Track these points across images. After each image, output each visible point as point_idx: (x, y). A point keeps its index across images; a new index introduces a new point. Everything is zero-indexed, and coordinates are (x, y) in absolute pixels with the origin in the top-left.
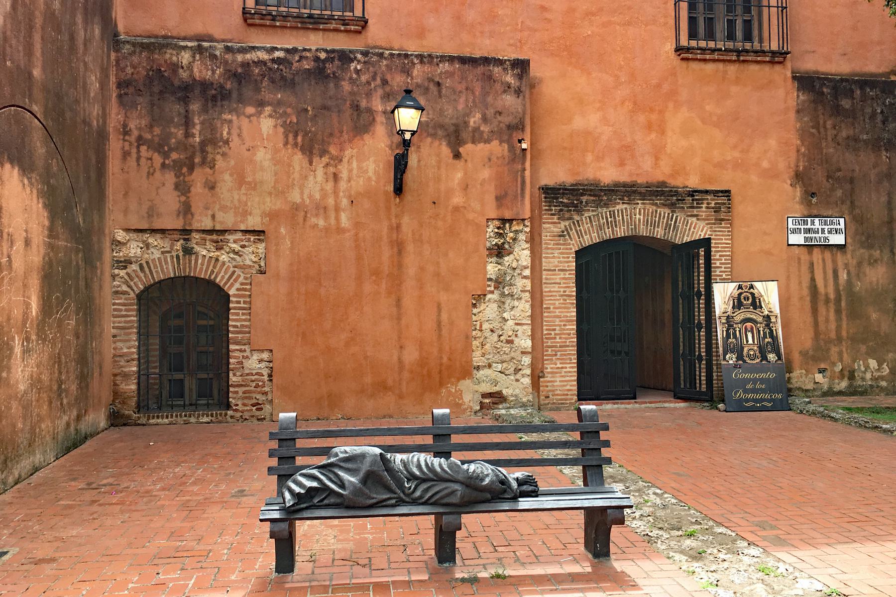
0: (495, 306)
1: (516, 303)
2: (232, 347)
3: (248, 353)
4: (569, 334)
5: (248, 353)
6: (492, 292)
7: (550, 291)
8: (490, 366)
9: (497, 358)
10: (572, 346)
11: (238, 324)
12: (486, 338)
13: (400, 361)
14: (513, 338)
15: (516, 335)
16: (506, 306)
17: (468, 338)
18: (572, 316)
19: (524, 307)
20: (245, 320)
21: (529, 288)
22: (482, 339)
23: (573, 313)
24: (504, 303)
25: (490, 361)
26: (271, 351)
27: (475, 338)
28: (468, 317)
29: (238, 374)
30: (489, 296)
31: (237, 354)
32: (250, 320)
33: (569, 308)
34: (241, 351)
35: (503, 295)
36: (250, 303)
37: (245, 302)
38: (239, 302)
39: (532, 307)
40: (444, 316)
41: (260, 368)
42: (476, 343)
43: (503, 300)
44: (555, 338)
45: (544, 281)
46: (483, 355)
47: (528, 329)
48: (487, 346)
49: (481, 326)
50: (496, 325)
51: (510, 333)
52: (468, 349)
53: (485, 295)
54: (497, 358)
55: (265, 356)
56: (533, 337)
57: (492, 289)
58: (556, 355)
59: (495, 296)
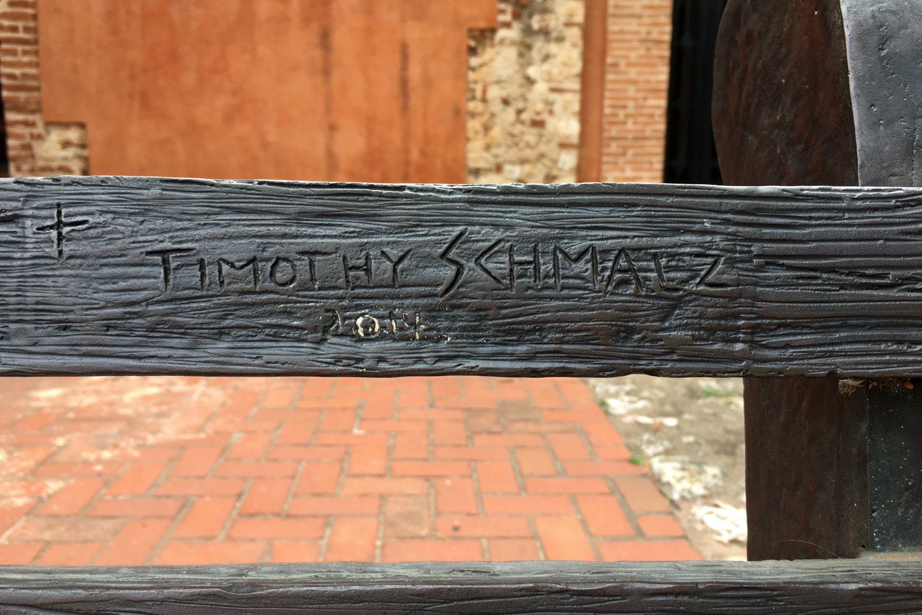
0: (511, 53)
1: (553, 48)
2: (10, 116)
3: (40, 129)
4: (652, 116)
5: (40, 129)
6: (507, 25)
7: (621, 32)
8: (499, 169)
9: (513, 153)
10: (657, 138)
11: (17, 72)
12: (493, 115)
13: (330, 155)
14: (545, 116)
15: (551, 112)
16: (535, 54)
17: (459, 115)
18: (659, 82)
19: (567, 56)
20: (29, 65)
21: (579, 18)
22: (485, 118)
23: (662, 75)
24: (529, 47)
25: (500, 160)
26: (82, 126)
27: (473, 115)
28: (461, 72)
29: (25, 167)
30: (502, 33)
31: (19, 130)
32: (36, 65)
33: (654, 65)
34: (26, 124)
35: (528, 31)
36: (35, 30)
37: (27, 30)
38: (14, 29)
39: (586, 59)
40: (415, 71)
41: (65, 159)
42: (474, 125)
43: (528, 41)
44: (624, 123)
45: (611, 10)
46: (488, 147)
47: (574, 101)
48: (496, 132)
49: (484, 91)
50: (512, 90)
51: (540, 106)
52: (459, 136)
53: (493, 31)
54: (513, 153)
55: (73, 135)
56: (583, 116)
57: (507, 17)
58: (624, 154)
59: (512, 34)
